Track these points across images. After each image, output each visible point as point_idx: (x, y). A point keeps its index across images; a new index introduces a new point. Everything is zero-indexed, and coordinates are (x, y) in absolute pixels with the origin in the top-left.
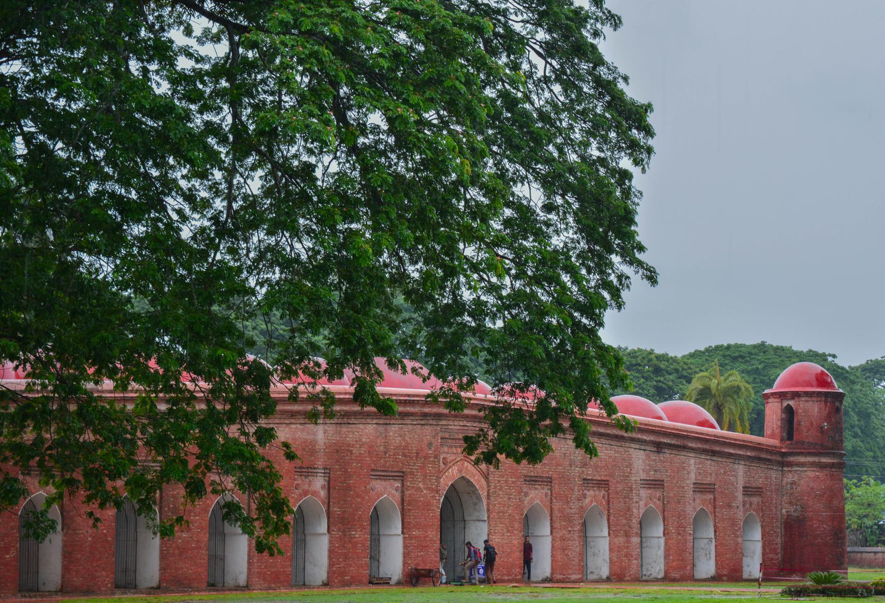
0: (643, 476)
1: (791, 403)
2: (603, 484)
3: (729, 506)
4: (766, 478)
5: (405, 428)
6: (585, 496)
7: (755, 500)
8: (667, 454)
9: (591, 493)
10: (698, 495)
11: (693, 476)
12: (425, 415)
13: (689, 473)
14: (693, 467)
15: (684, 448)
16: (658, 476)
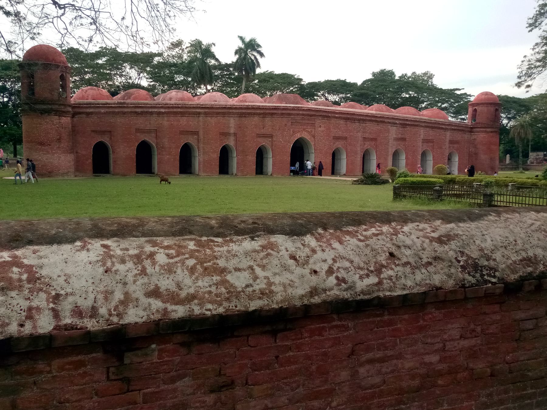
0: (395, 136)
1: (476, 108)
2: (374, 139)
3: (441, 148)
4: (462, 137)
5: (273, 119)
6: (365, 144)
7: (456, 146)
8: (408, 128)
9: (368, 143)
10: (425, 144)
11: (422, 136)
12: (282, 114)
13: (420, 135)
14: (422, 133)
15: (417, 126)
16: (403, 136)
